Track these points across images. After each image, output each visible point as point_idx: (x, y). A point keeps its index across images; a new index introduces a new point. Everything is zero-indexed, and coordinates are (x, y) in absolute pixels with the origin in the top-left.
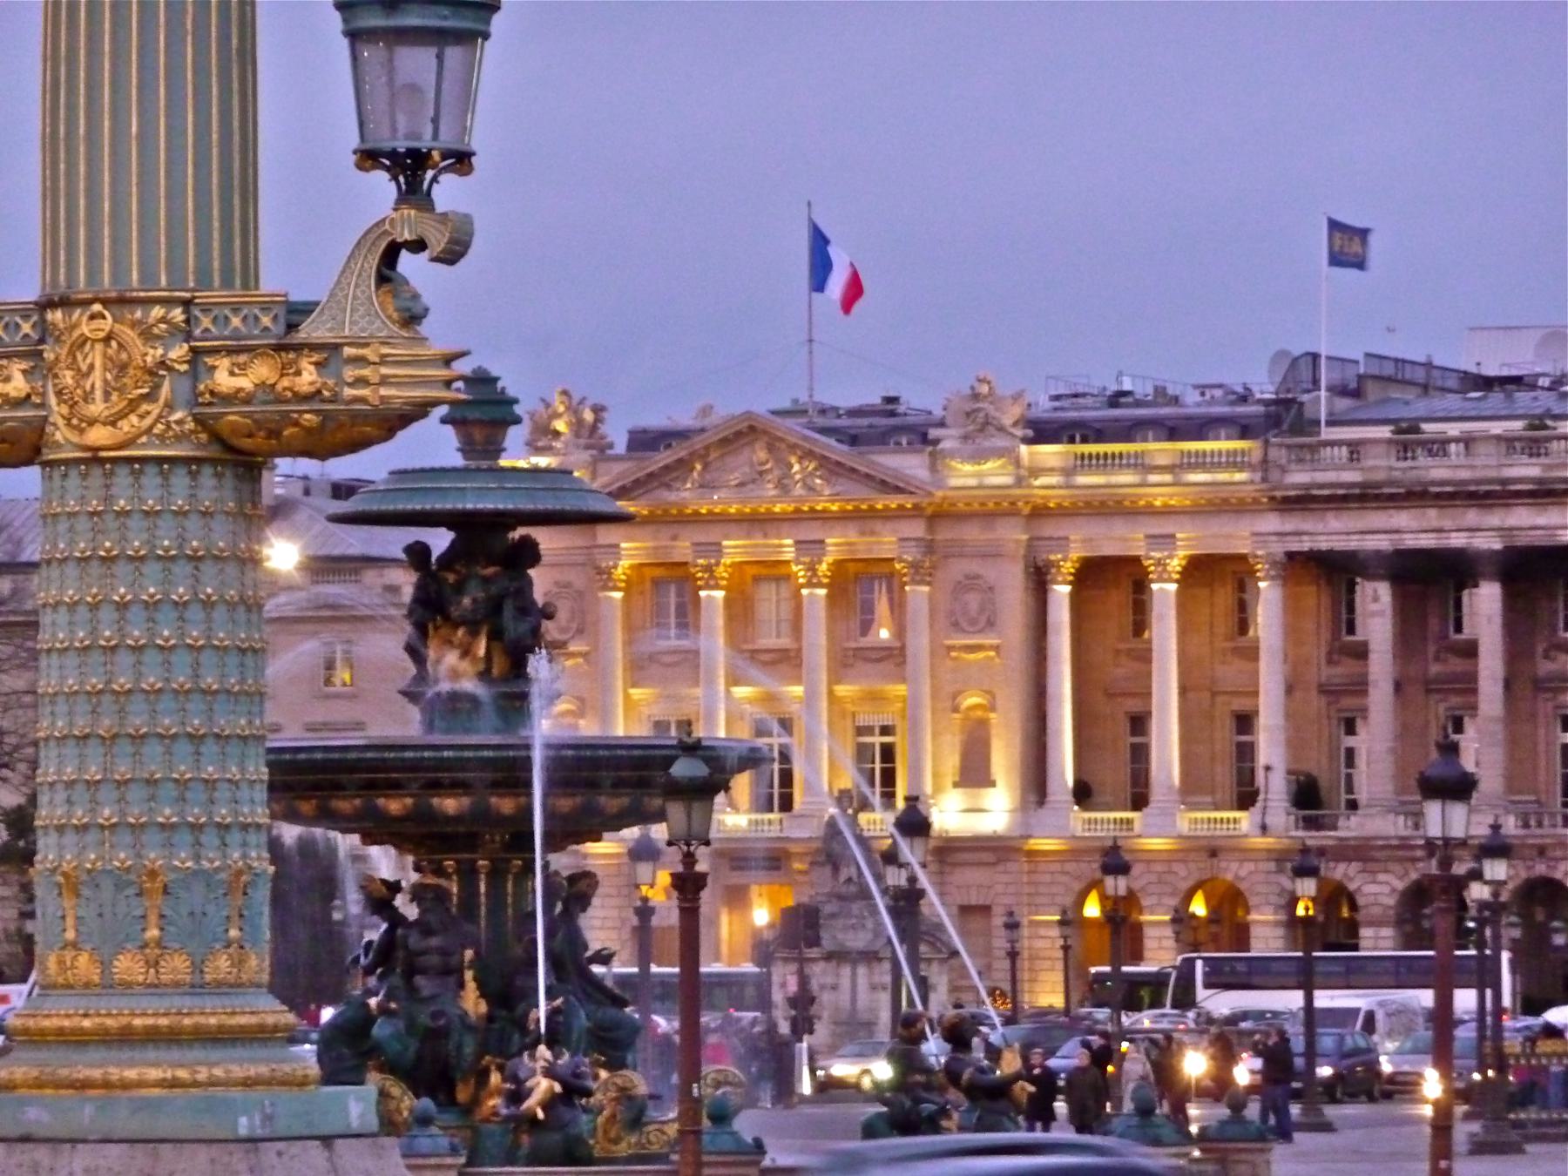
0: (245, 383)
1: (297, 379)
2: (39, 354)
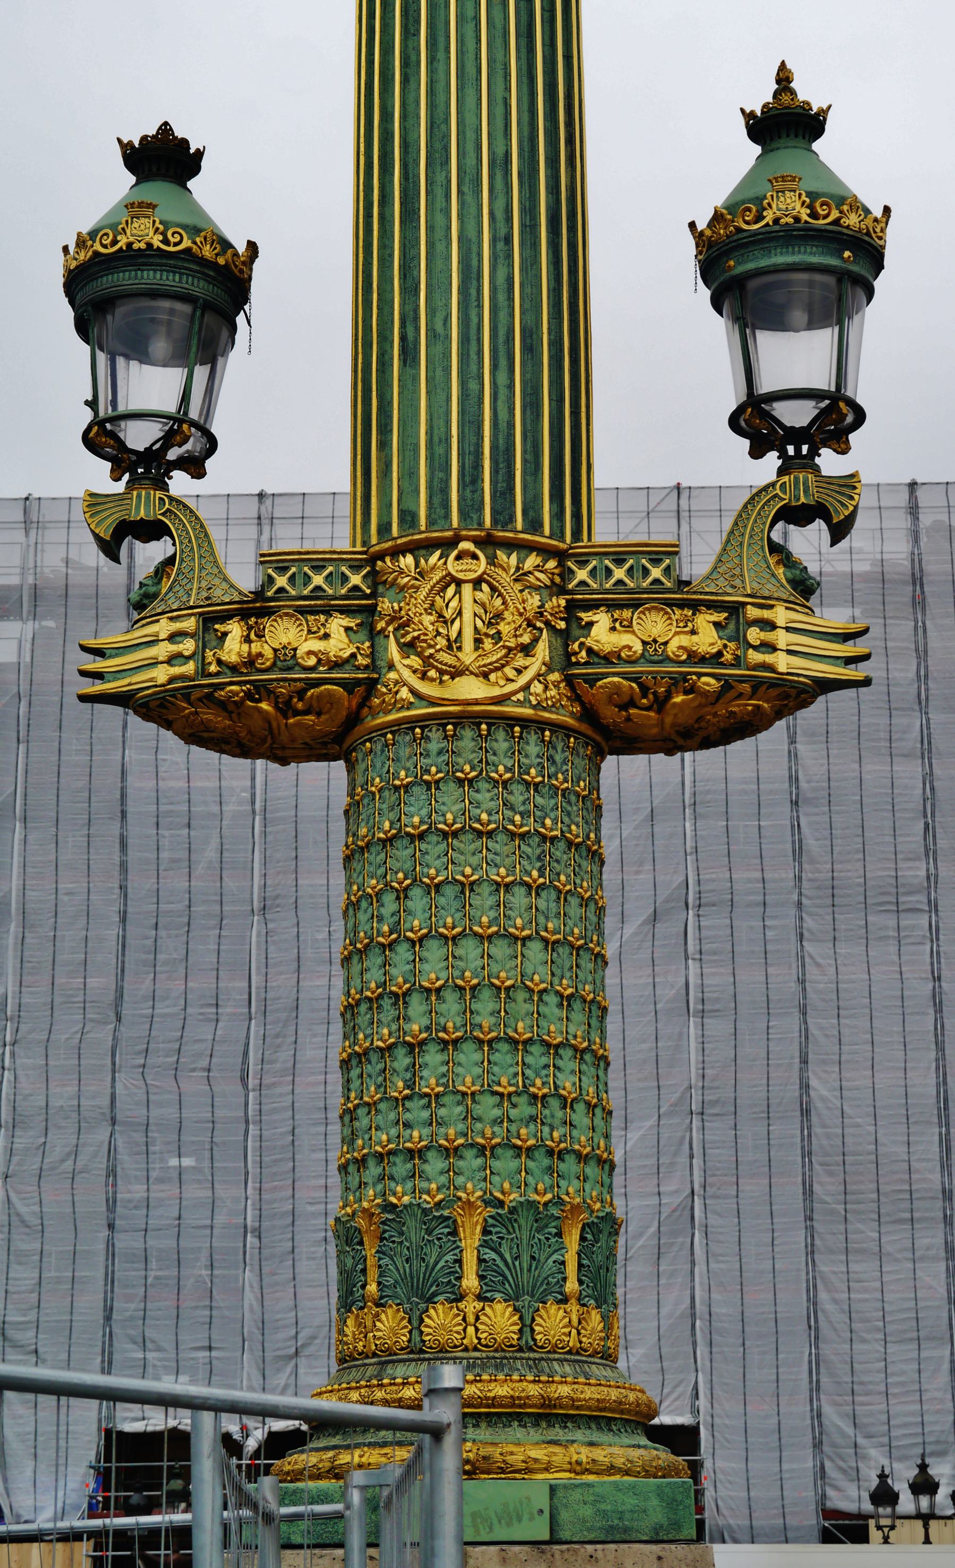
0: (631, 642)
1: (694, 637)
2: (371, 610)
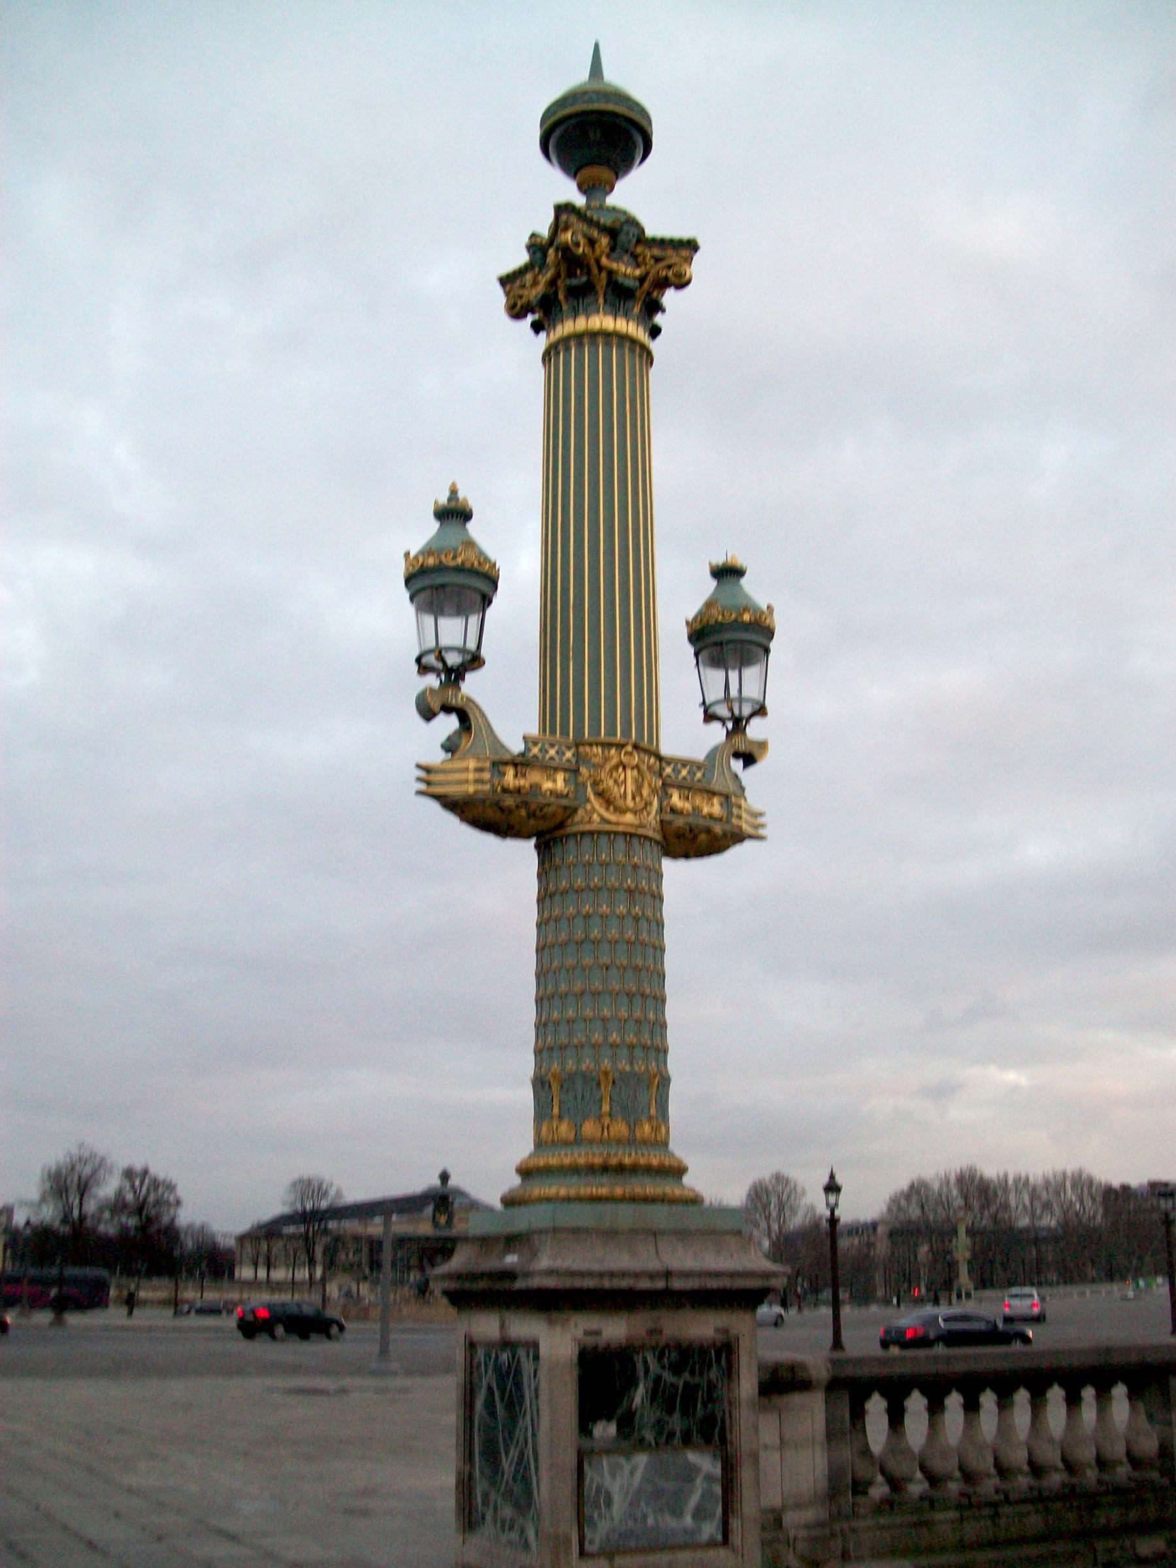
0: (687, 806)
2: (576, 771)
